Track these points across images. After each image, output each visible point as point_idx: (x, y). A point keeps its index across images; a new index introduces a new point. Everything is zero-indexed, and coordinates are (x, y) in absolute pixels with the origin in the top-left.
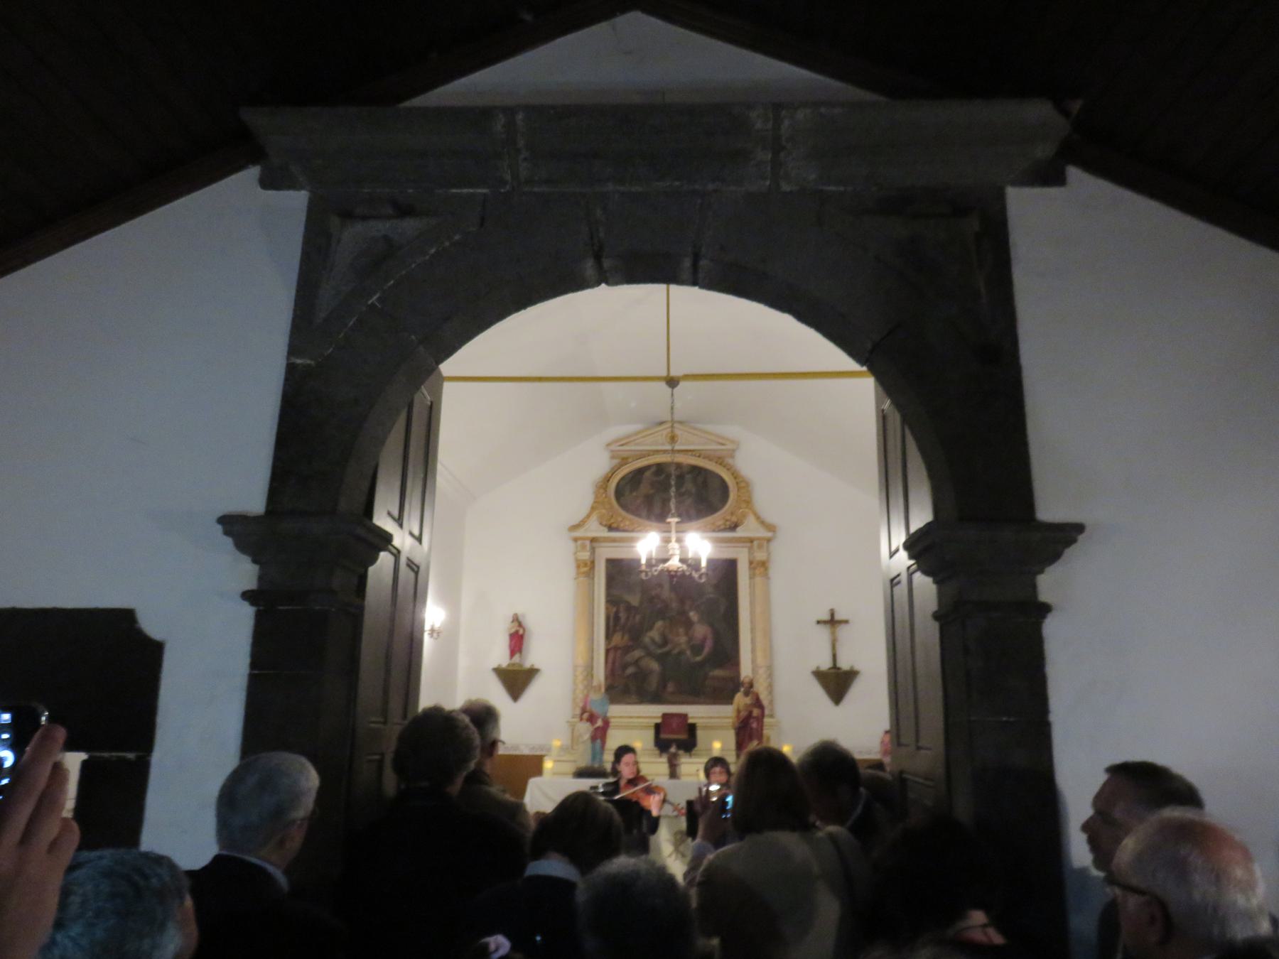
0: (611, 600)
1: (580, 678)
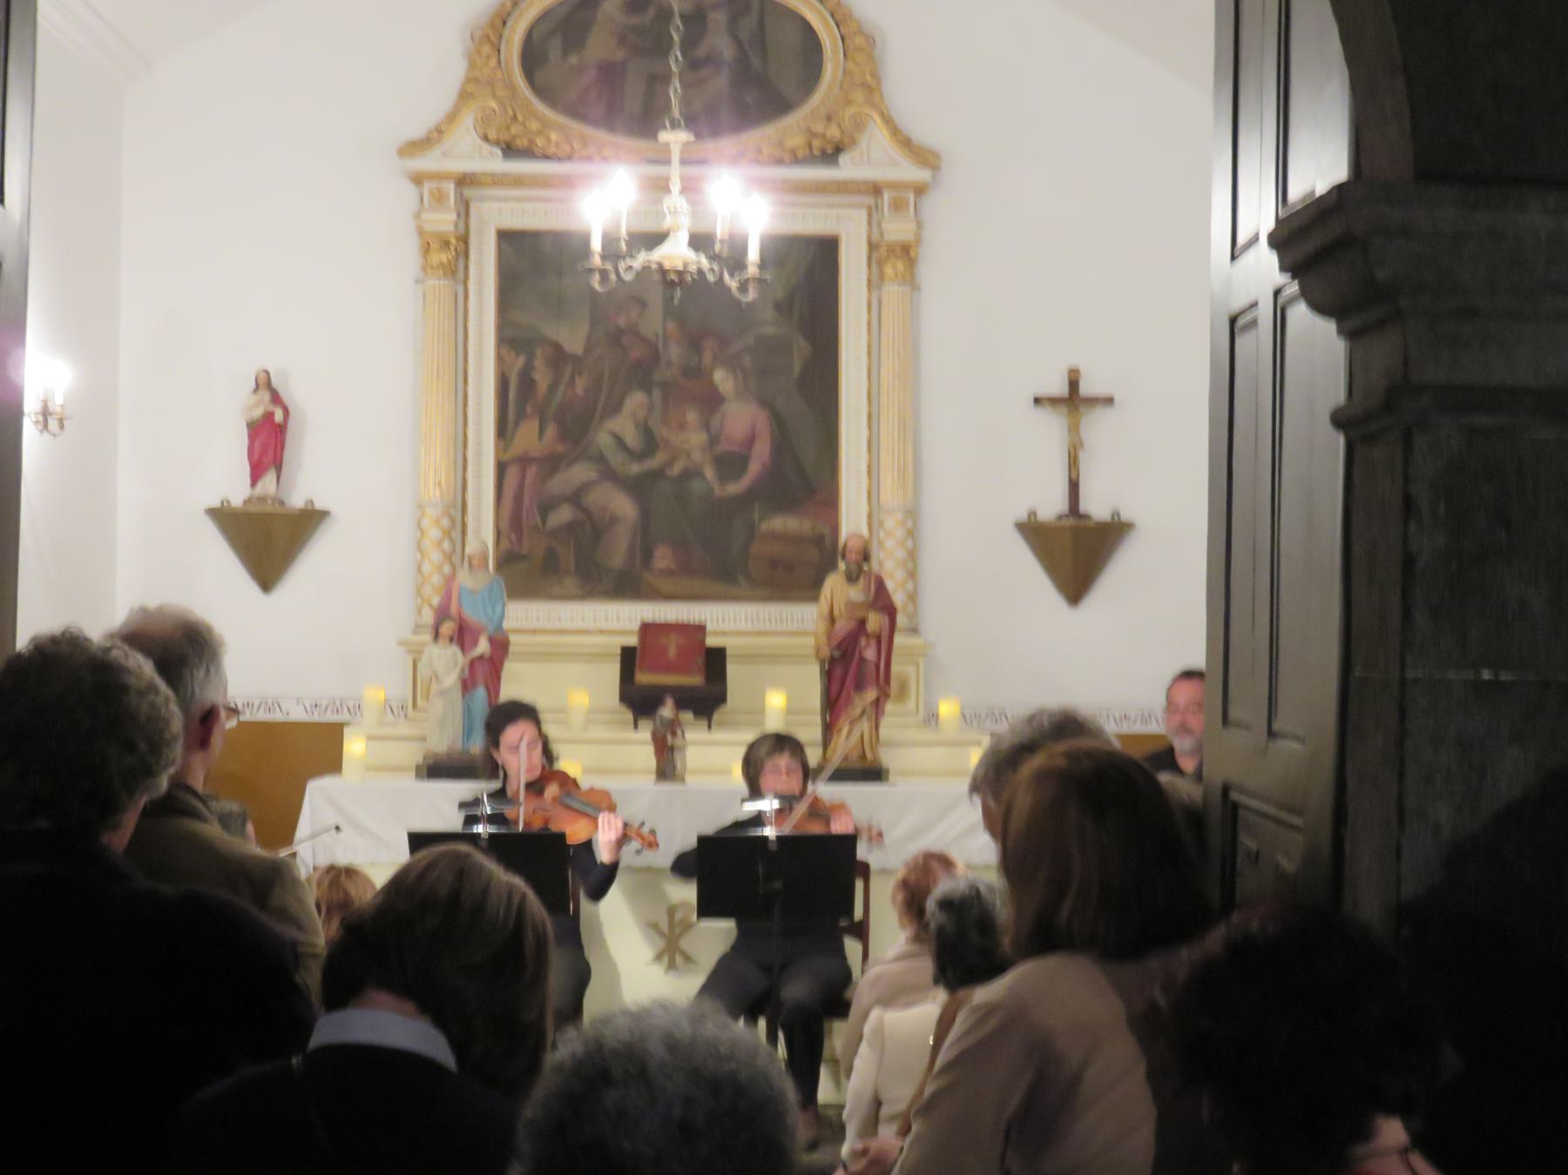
0: (511, 338)
1: (434, 533)
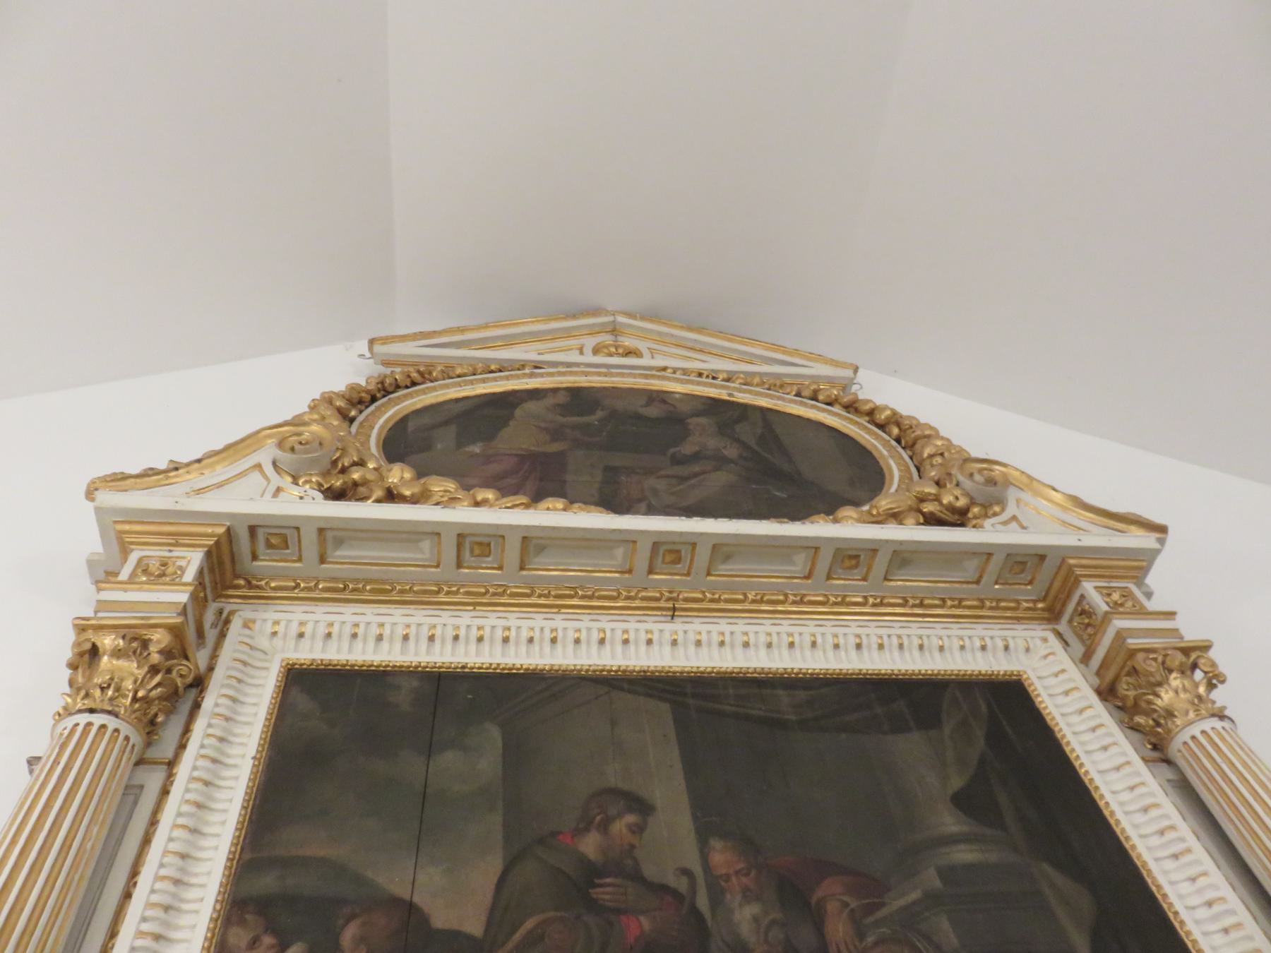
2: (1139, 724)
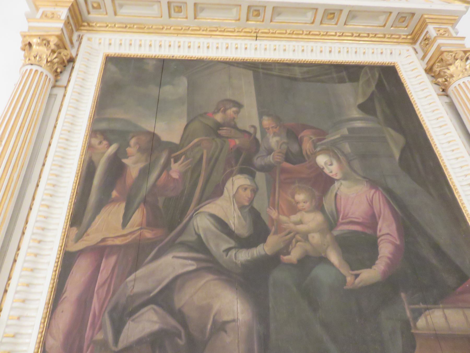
0: (101, 129)
2: (439, 82)
